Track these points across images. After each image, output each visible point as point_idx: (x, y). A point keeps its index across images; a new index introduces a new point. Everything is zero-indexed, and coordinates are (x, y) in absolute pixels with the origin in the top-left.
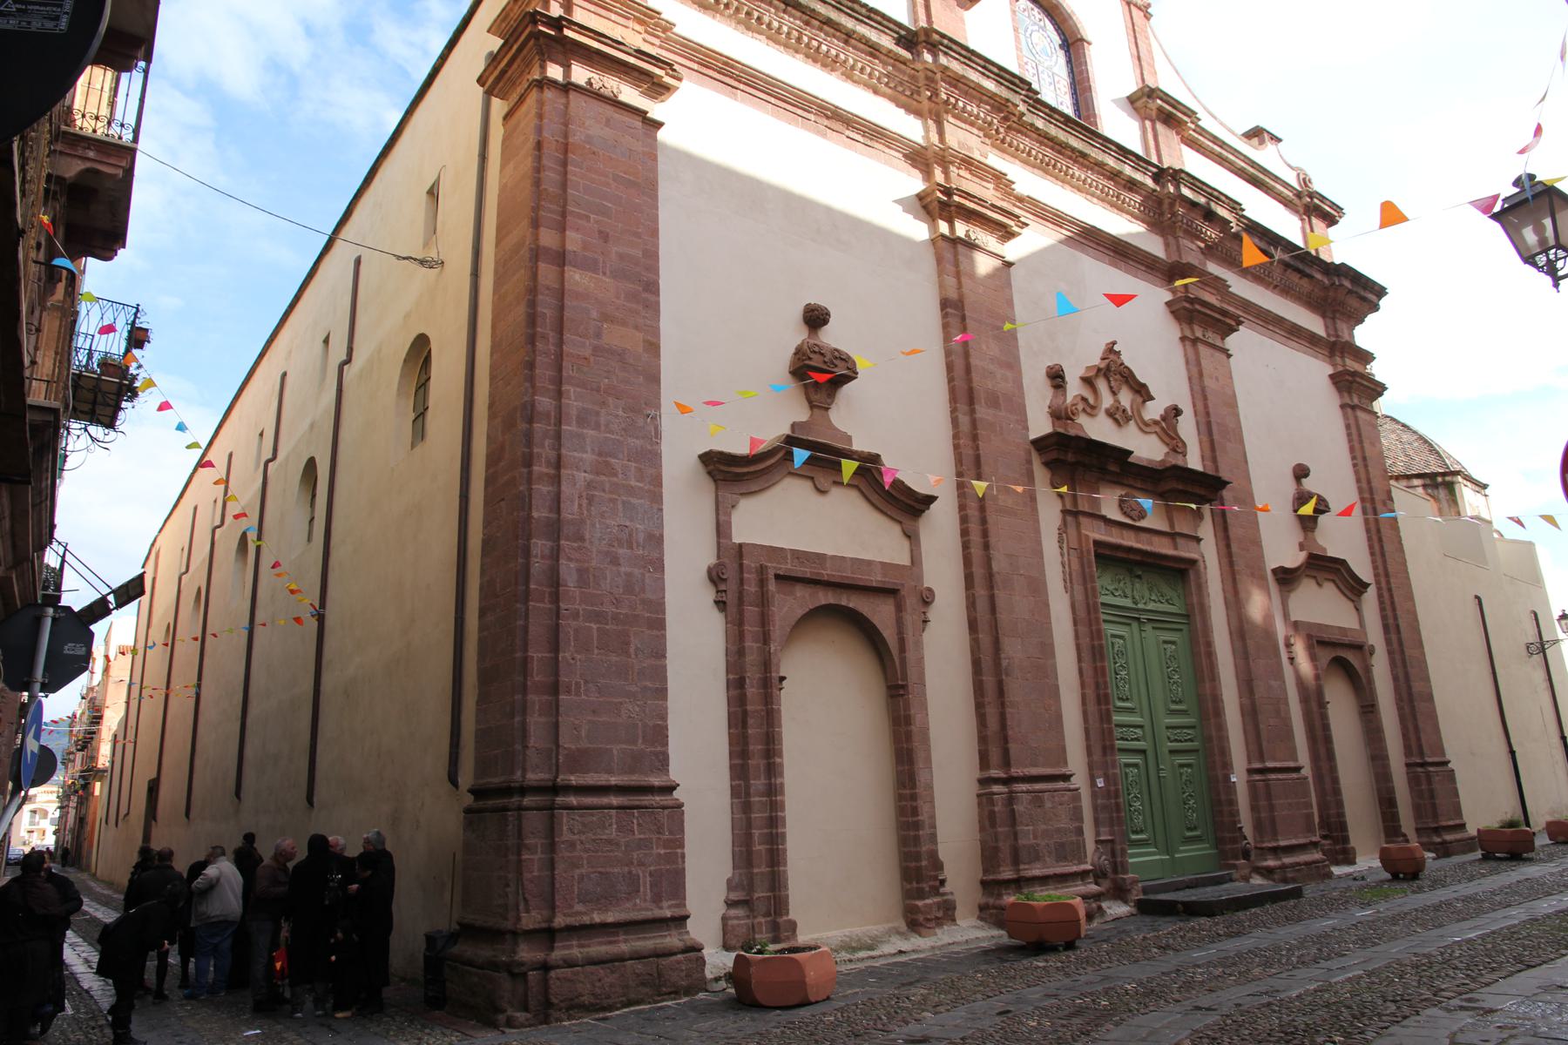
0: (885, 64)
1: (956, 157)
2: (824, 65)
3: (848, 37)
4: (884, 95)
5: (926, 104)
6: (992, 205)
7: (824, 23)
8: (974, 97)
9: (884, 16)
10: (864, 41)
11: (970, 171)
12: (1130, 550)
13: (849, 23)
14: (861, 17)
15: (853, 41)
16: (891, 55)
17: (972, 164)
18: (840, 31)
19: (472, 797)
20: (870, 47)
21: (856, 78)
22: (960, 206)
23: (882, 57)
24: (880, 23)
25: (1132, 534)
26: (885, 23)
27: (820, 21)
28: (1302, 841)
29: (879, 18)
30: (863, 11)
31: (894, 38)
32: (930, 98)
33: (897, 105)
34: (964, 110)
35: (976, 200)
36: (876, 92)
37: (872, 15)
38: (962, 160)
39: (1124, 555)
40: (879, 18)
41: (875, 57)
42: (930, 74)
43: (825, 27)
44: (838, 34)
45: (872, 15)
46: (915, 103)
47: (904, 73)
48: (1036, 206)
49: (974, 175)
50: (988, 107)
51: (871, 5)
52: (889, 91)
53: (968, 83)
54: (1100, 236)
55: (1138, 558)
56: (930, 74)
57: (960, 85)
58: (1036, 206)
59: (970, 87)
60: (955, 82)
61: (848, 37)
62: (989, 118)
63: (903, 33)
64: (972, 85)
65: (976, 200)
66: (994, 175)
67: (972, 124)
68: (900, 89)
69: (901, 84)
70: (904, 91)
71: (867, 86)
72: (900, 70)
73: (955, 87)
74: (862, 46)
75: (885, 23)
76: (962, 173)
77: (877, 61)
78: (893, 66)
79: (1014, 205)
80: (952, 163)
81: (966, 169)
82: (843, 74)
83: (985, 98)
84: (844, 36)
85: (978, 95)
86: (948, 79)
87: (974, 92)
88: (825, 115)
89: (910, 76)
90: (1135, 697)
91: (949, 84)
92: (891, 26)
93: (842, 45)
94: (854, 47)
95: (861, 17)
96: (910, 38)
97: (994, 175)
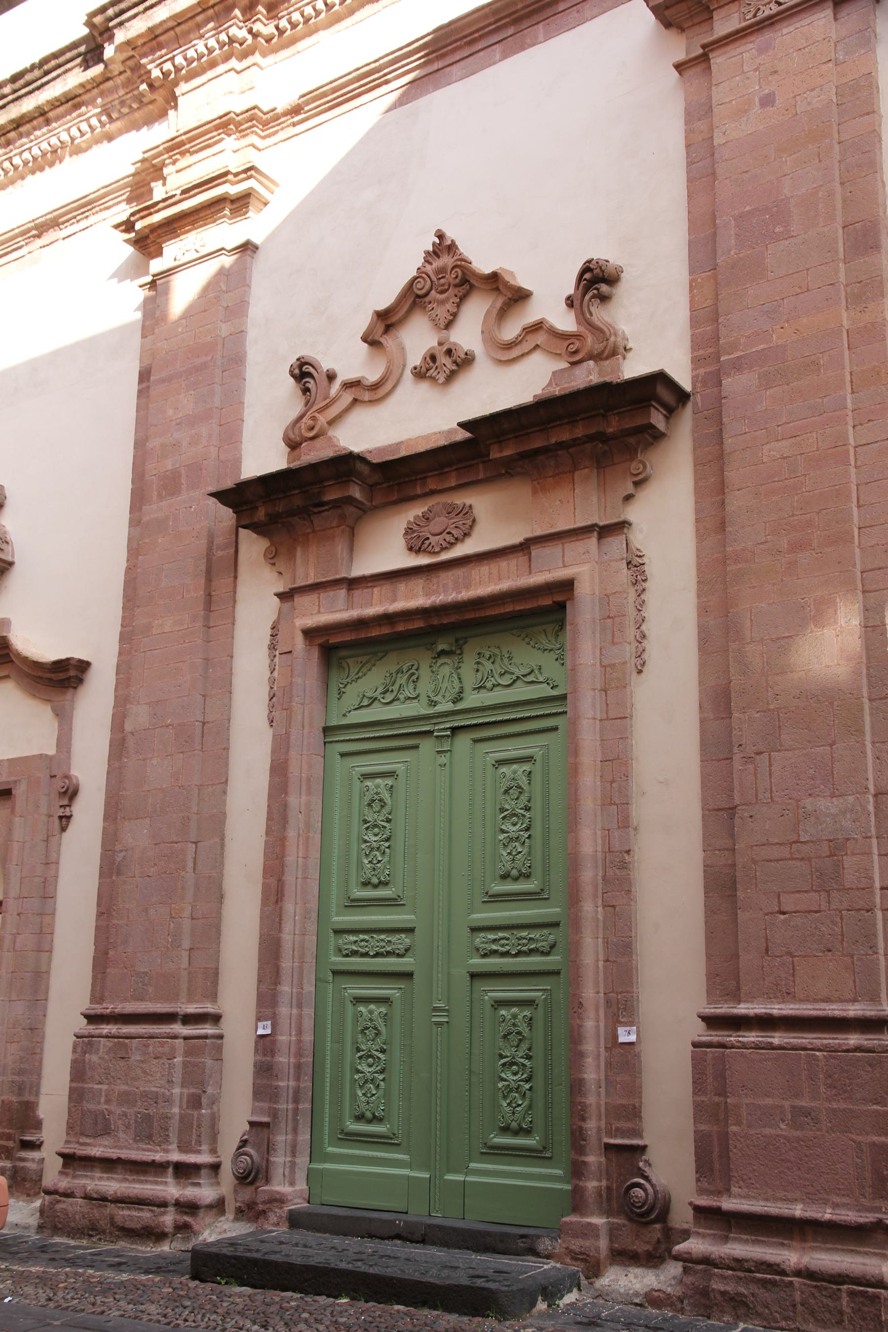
0: (91, 102)
1: (160, 154)
2: (51, 164)
3: (42, 116)
4: (121, 132)
5: (159, 96)
6: (184, 192)
7: (18, 127)
8: (188, 32)
9: (55, 56)
10: (58, 104)
11: (188, 151)
12: (388, 618)
13: (28, 105)
14: (39, 83)
15: (51, 115)
16: (89, 87)
17: (182, 144)
18: (35, 118)
19: (85, 1021)
20: (67, 101)
21: (84, 145)
22: (154, 229)
23: (85, 97)
24: (59, 66)
25: (418, 583)
26: (62, 59)
27: (15, 129)
28: (850, 1216)
29: (53, 63)
30: (37, 73)
31: (80, 65)
32: (151, 86)
33: (138, 128)
34: (190, 61)
35: (161, 205)
36: (110, 138)
37: (46, 67)
38: (169, 150)
39: (386, 630)
40: (53, 63)
41: (77, 107)
42: (130, 63)
43: (22, 129)
44: (35, 122)
45: (46, 67)
46: (151, 107)
47: (116, 89)
48: (324, 95)
49: (197, 152)
50: (211, 25)
51: (36, 60)
52: (118, 124)
53: (166, 26)
54: (462, 28)
55: (419, 624)
56: (130, 63)
57: (162, 38)
58: (324, 95)
59: (172, 28)
60: (154, 43)
61: (42, 116)
62: (223, 37)
63: (82, 49)
64: (171, 24)
65: (161, 205)
66: (217, 128)
67: (213, 64)
68: (125, 110)
69: (123, 103)
70: (131, 107)
71: (98, 141)
72: (111, 91)
73: (160, 47)
74: (61, 110)
75: (62, 59)
76: (182, 164)
77: (84, 109)
78: (102, 94)
79: (294, 125)
80: (164, 164)
81: (182, 154)
82: (71, 156)
83: (199, 19)
84: (41, 119)
85: (190, 24)
86: (145, 49)
87: (184, 27)
88: (34, 236)
89: (125, 85)
90: (538, 871)
91: (153, 51)
92: (69, 55)
93: (45, 130)
94: (58, 118)
95: (39, 83)
96: (93, 46)
97: (217, 128)
